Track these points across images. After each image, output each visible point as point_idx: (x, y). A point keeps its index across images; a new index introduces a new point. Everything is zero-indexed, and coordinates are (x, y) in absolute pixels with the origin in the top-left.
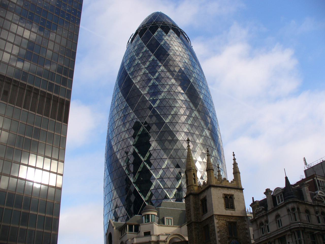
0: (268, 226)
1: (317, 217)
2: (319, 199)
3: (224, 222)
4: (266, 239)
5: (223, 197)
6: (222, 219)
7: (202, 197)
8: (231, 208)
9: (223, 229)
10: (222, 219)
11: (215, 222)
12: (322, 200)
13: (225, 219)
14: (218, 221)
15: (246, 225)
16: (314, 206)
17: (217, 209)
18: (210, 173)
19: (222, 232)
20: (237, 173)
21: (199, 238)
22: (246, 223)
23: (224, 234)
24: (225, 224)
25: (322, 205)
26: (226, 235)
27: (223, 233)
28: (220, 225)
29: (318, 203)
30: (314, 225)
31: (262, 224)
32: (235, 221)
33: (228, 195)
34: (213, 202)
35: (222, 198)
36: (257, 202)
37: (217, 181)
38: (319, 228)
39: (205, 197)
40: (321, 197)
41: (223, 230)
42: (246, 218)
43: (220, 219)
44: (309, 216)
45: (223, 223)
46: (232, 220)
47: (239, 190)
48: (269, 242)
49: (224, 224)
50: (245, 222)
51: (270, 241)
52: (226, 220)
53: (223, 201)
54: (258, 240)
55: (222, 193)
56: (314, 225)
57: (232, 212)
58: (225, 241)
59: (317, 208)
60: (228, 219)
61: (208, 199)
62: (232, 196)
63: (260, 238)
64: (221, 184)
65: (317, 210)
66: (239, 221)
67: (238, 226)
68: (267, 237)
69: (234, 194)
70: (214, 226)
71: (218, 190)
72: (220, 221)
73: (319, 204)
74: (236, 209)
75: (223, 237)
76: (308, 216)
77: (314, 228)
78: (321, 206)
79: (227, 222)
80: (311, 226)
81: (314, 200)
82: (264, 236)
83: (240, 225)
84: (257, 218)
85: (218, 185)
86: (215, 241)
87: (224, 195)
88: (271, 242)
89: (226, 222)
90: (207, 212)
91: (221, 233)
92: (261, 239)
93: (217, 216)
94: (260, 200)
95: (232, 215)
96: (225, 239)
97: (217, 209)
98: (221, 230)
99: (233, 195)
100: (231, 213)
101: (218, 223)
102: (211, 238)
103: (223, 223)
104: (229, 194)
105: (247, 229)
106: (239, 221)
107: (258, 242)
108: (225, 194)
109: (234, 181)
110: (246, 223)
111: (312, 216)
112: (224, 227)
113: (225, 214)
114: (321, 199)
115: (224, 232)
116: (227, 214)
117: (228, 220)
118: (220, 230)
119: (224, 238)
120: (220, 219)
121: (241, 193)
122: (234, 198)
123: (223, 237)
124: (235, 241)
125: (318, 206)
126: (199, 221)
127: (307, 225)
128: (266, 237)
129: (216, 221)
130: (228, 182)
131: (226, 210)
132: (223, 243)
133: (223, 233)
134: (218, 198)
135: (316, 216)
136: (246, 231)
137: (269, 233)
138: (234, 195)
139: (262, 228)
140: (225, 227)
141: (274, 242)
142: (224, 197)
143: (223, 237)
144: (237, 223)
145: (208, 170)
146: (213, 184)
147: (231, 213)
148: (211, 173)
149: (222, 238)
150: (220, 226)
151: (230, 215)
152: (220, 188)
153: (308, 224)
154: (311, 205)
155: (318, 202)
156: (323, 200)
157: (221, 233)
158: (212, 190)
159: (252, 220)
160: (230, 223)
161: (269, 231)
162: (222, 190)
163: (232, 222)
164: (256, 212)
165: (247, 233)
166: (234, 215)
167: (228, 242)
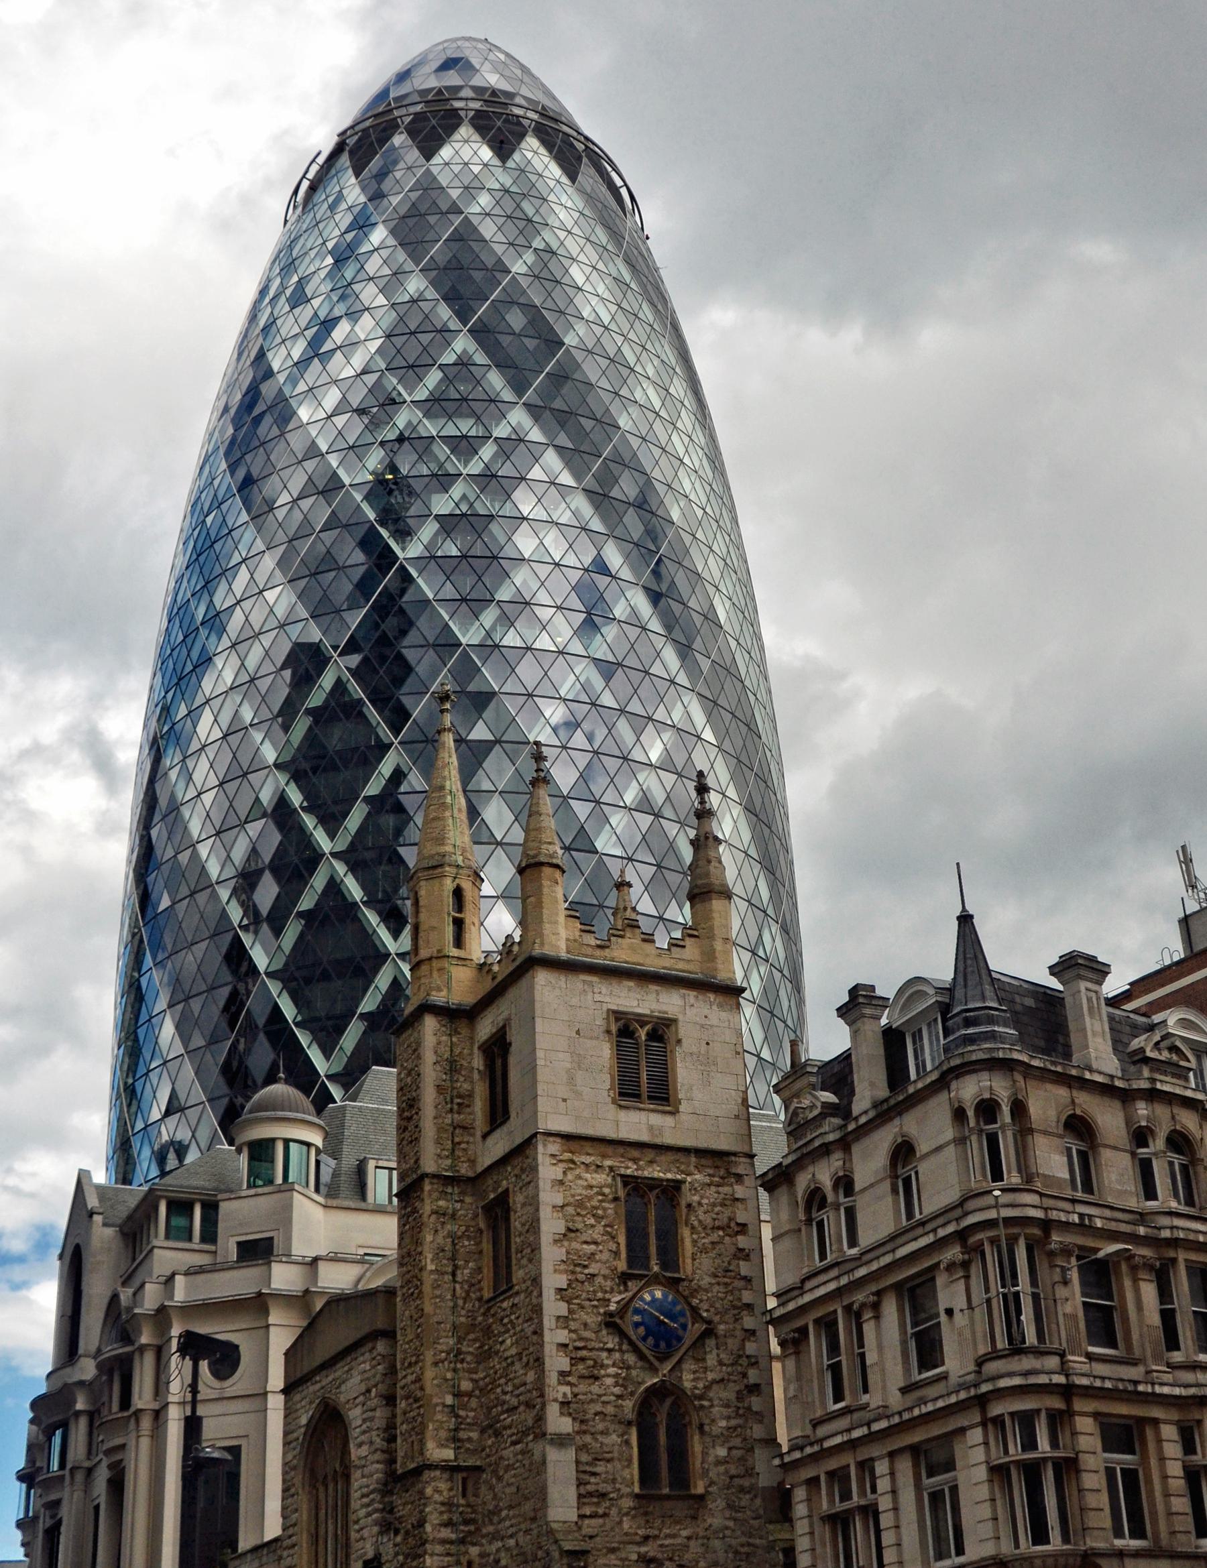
0: (851, 1214)
1: (1141, 1160)
2: (1165, 1055)
3: (601, 1178)
4: (832, 1286)
5: (608, 1032)
6: (588, 1160)
7: (485, 1028)
8: (650, 1098)
9: (592, 1221)
10: (588, 1160)
11: (541, 1175)
12: (1183, 1063)
13: (608, 1163)
14: (564, 1173)
15: (739, 1204)
16: (1126, 1097)
17: (564, 1100)
18: (540, 887)
19: (585, 1237)
20: (709, 892)
21: (454, 1274)
22: (740, 1191)
23: (593, 1254)
24: (607, 1191)
25: (1178, 1091)
26: (605, 1256)
27: (593, 1247)
28: (573, 1196)
29: (1153, 1081)
30: (1112, 1208)
31: (815, 1199)
32: (669, 1176)
33: (641, 1020)
34: (540, 1054)
35: (601, 1036)
36: (809, 1069)
37: (577, 933)
38: (1142, 1231)
39: (504, 1027)
40: (1178, 1043)
41: (593, 1226)
42: (742, 1160)
43: (576, 1159)
44: (1090, 1153)
45: (594, 1183)
46: (655, 1172)
47: (712, 996)
48: (848, 1309)
49: (603, 1195)
50: (737, 1188)
51: (852, 1304)
52: (611, 1168)
53: (604, 1052)
54: (796, 1293)
55: (605, 1009)
56: (1112, 1208)
57: (656, 1119)
58: (600, 1295)
59: (1142, 1110)
60: (630, 1164)
61: (515, 1037)
62: (668, 1026)
63: (803, 1281)
64: (607, 952)
65: (1144, 1123)
66: (698, 1177)
67: (689, 1206)
68: (837, 1278)
69: (680, 1017)
70: (533, 1203)
71: (580, 985)
72: (577, 1172)
73: (1159, 1086)
74: (682, 1108)
75: (586, 1271)
76: (1083, 1156)
77: (1113, 1226)
78: (1170, 1099)
79: (619, 1179)
80: (1090, 1216)
81: (1134, 1063)
82: (826, 1270)
83: (705, 1201)
84: (793, 1162)
85: (586, 956)
86: (535, 1293)
87: (617, 1020)
88: (855, 1307)
89: (614, 1178)
90: (509, 1118)
91: (575, 1245)
92: (809, 1285)
93: (559, 1140)
94: (827, 1058)
95: (658, 1141)
96: (599, 1280)
97: (564, 1100)
98: (580, 1226)
99: (669, 1019)
100: (651, 1128)
101: (561, 1182)
102: (521, 1273)
103: (591, 1187)
104: (647, 1012)
105: (743, 1228)
106: (698, 1177)
107: (791, 1306)
108: (618, 1015)
109: (689, 942)
110: (740, 1191)
111: (1106, 1155)
112: (600, 1212)
113: (611, 1134)
114: (1175, 1057)
115: (596, 1243)
116: (625, 1134)
117: (629, 1172)
118: (569, 1230)
119: (594, 1275)
120: (573, 1162)
121: (724, 1015)
122: (679, 1041)
123: (585, 1267)
124: (658, 1294)
125: (1153, 1095)
126: (464, 1170)
127: (1067, 1206)
128: (834, 1273)
129: (548, 1171)
130: (647, 946)
131: (621, 1107)
132: (588, 1303)
133: (586, 1242)
134: (578, 1032)
135: (1133, 1154)
136: (740, 1238)
137: (854, 1251)
138: (680, 1024)
139: (820, 1225)
140: (605, 1209)
141: (876, 1306)
142: (614, 1029)
143: (586, 1271)
144: (685, 1188)
145: (528, 866)
146: (548, 951)
147: (651, 1128)
148: (546, 883)
149: (581, 1277)
150: (572, 1200)
151: (645, 1137)
152: (594, 979)
153: (1074, 1201)
154: (1107, 1090)
155: (1152, 1070)
156: (1188, 1061)
157: (575, 1245)
158: (538, 987)
159: (770, 1176)
160: (635, 1186)
161: (853, 1243)
162: (604, 991)
163: (653, 1184)
164: (792, 1127)
165: (742, 1250)
166: (668, 1140)
167: (618, 1303)
